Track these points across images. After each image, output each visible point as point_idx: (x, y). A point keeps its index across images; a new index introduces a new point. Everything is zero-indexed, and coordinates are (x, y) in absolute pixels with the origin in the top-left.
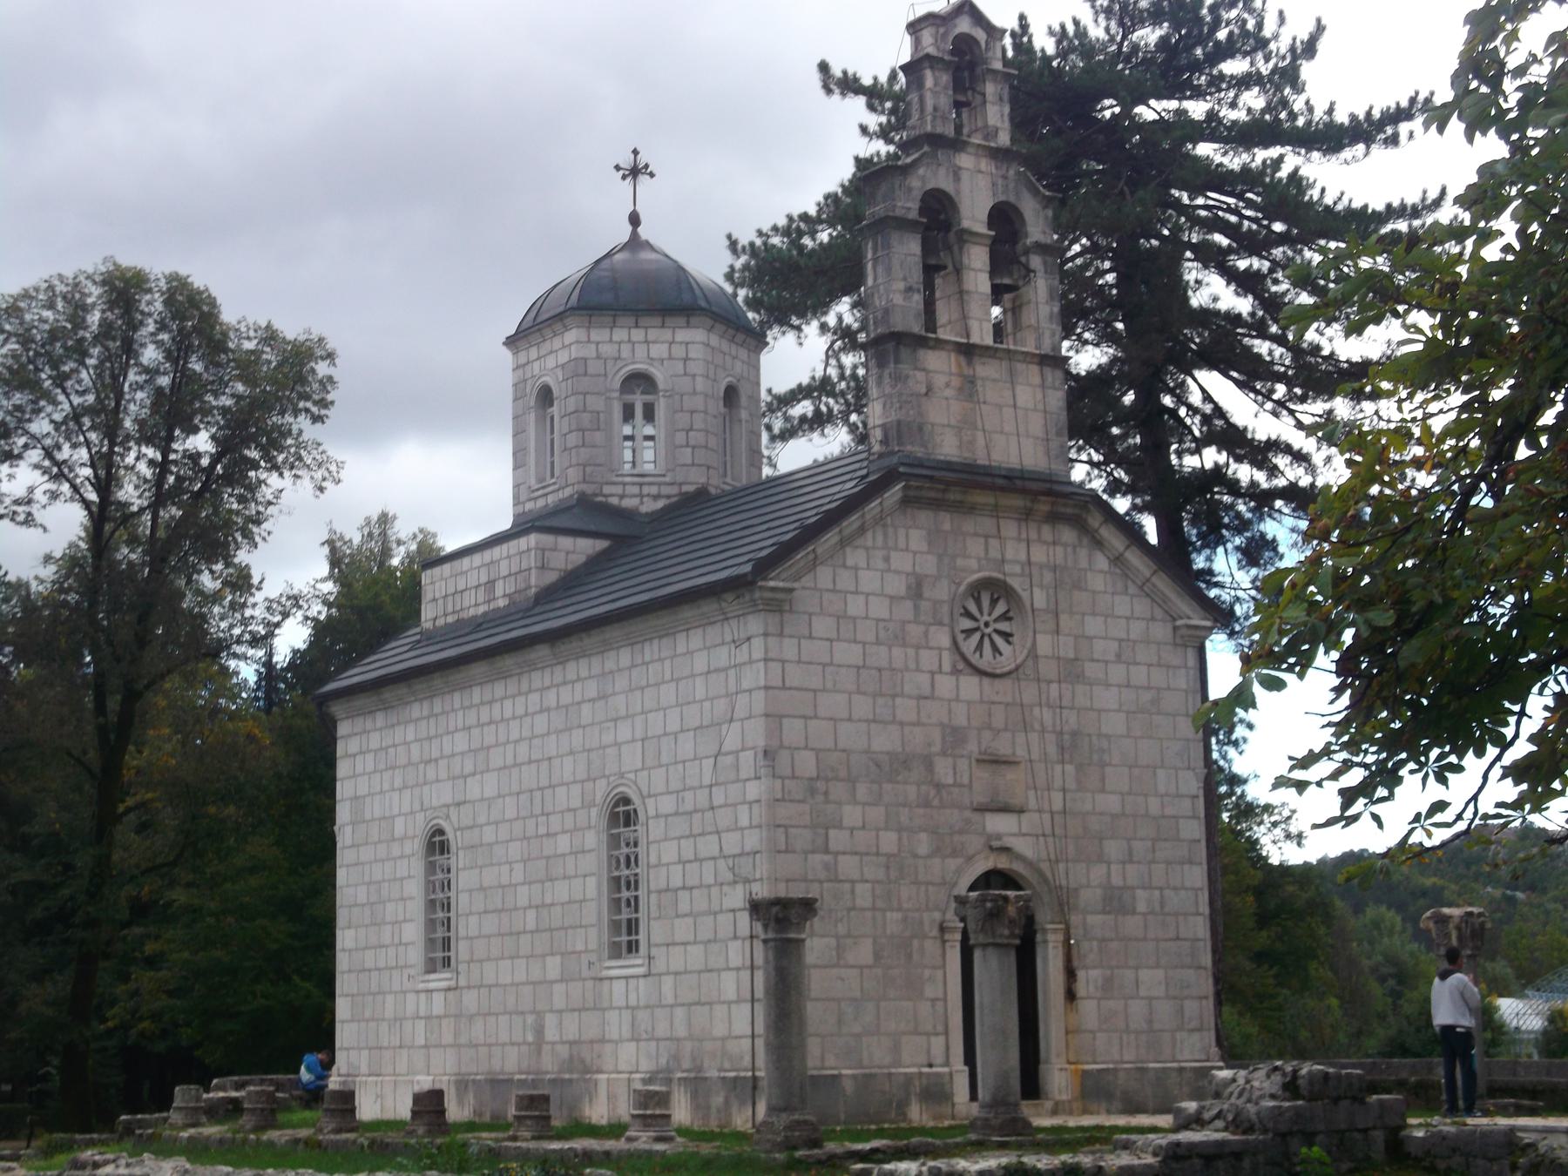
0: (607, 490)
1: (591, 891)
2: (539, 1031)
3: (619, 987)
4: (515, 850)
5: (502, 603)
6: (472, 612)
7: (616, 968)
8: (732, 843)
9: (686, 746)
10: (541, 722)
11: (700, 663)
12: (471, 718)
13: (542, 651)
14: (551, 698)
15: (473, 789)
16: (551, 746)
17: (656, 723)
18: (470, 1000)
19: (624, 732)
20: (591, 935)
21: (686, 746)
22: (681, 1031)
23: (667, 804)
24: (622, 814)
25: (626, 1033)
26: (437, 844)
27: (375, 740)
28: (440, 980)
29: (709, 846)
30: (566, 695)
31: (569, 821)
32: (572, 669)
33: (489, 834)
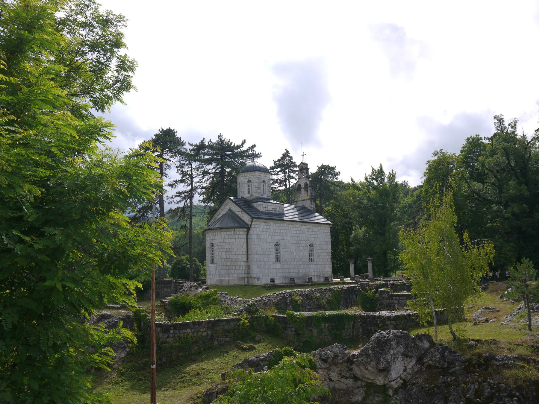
1: (307, 254)
2: (299, 271)
3: (312, 266)
4: (293, 247)
6: (272, 212)
7: (311, 263)
8: (327, 251)
9: (321, 240)
10: (298, 232)
11: (322, 231)
12: (284, 228)
14: (299, 229)
15: (285, 238)
16: (300, 235)
18: (285, 267)
19: (312, 236)
20: (307, 259)
21: (321, 240)
22: (321, 271)
23: (318, 246)
24: (311, 246)
25: (313, 271)
26: (277, 244)
27: (262, 227)
28: (278, 263)
29: (324, 251)
30: (302, 230)
31: (303, 245)
32: (303, 227)
33: (288, 245)
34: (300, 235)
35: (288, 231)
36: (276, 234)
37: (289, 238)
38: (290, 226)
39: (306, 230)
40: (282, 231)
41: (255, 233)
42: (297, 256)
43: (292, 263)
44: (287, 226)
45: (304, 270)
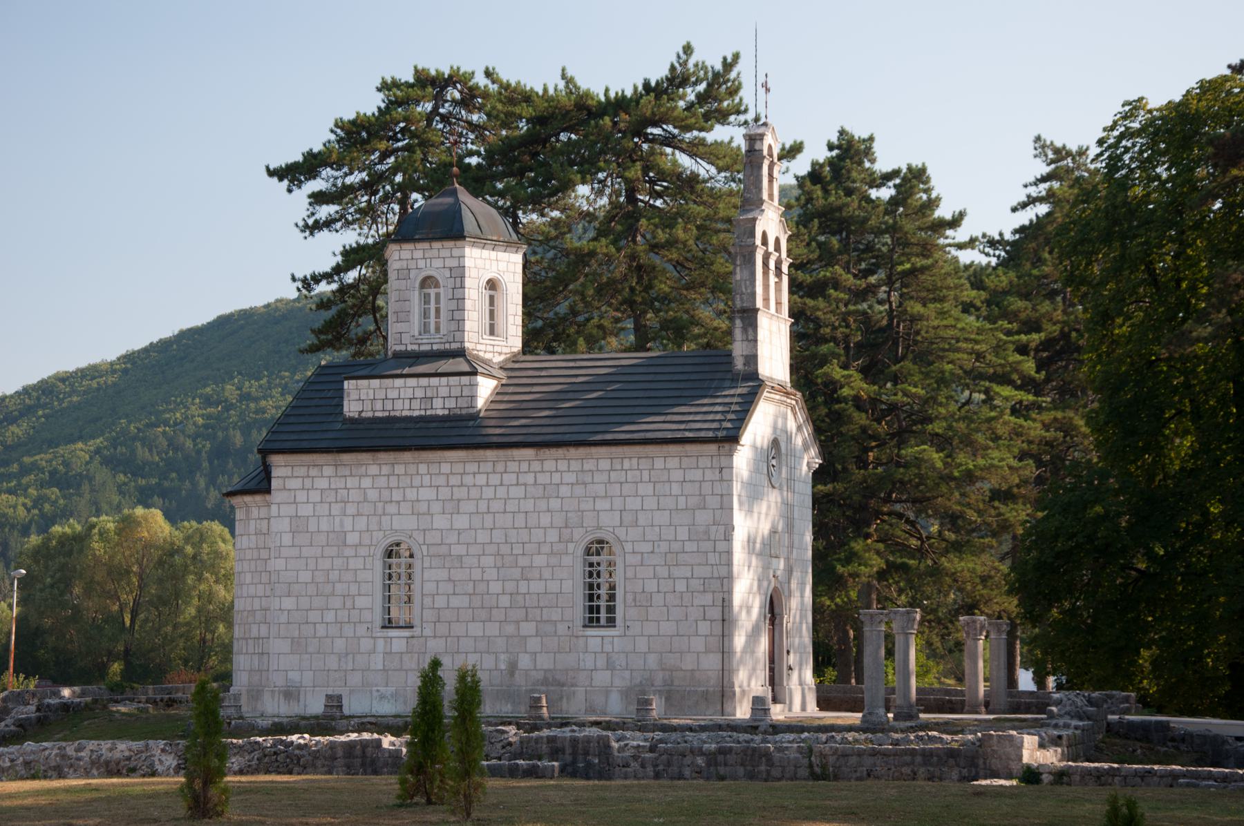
0: (479, 347)
5: (440, 412)
7: (591, 632)
13: (529, 453)
16: (528, 505)
17: (634, 504)
33: (458, 550)
34: (528, 505)
35: (460, 493)
36: (392, 509)
37: (461, 522)
38: (472, 467)
39: (570, 477)
40: (427, 494)
41: (287, 510)
42: (505, 601)
43: (476, 629)
44: (458, 468)
45: (545, 662)
